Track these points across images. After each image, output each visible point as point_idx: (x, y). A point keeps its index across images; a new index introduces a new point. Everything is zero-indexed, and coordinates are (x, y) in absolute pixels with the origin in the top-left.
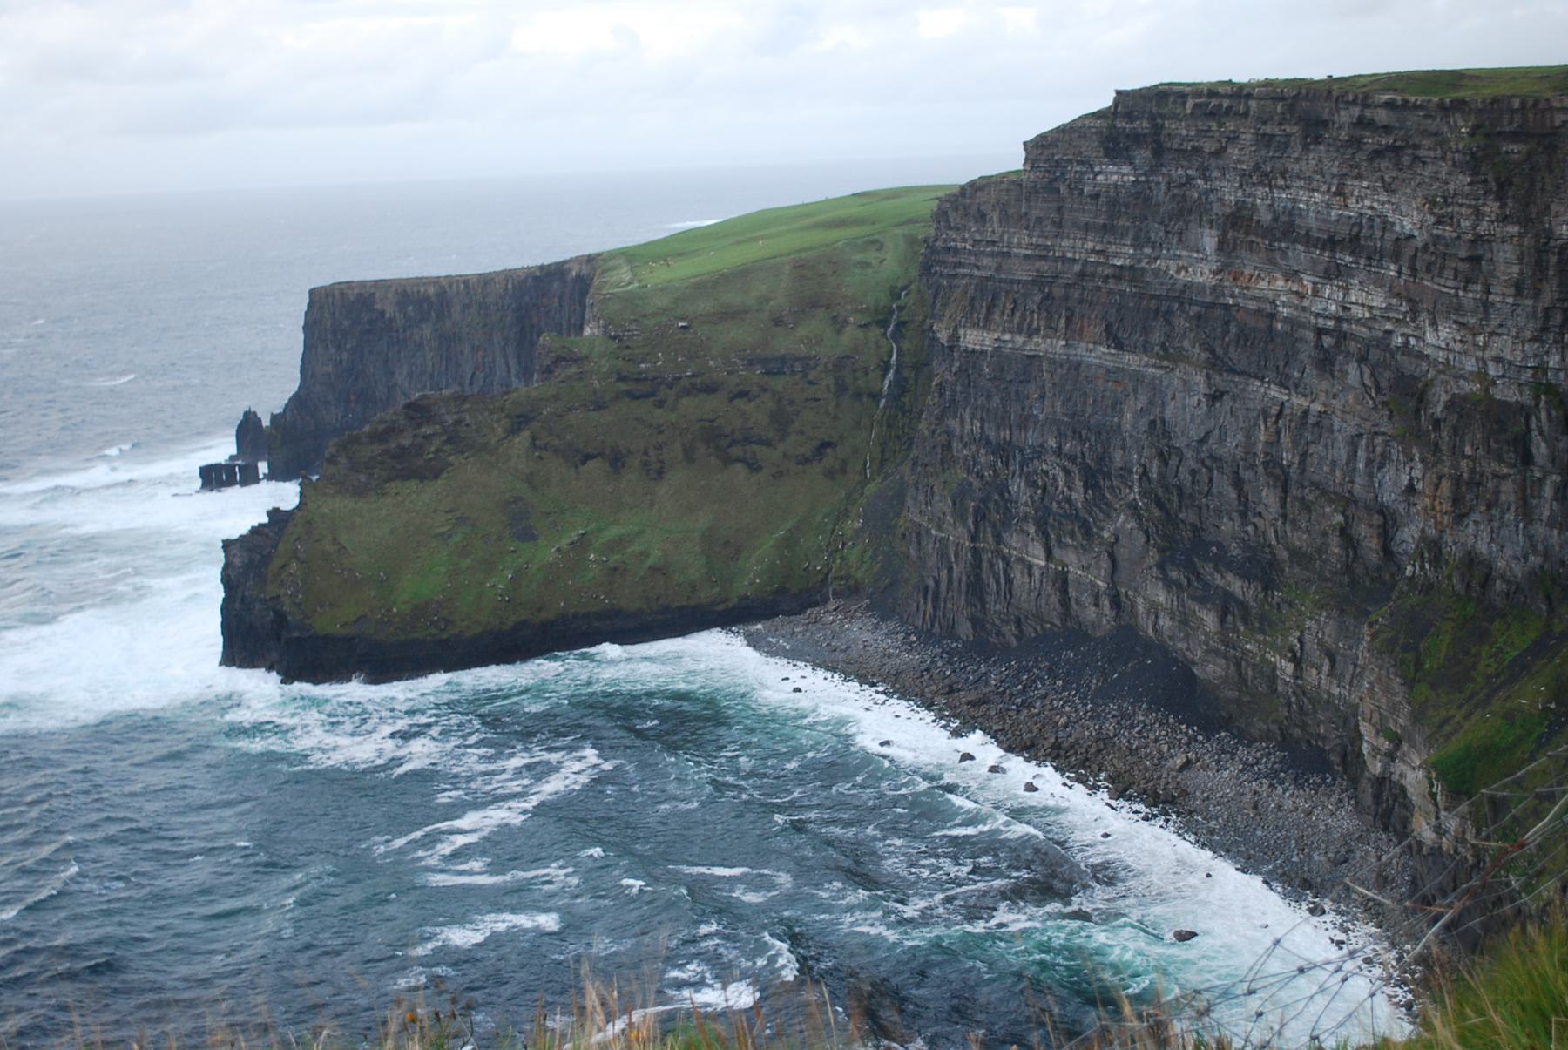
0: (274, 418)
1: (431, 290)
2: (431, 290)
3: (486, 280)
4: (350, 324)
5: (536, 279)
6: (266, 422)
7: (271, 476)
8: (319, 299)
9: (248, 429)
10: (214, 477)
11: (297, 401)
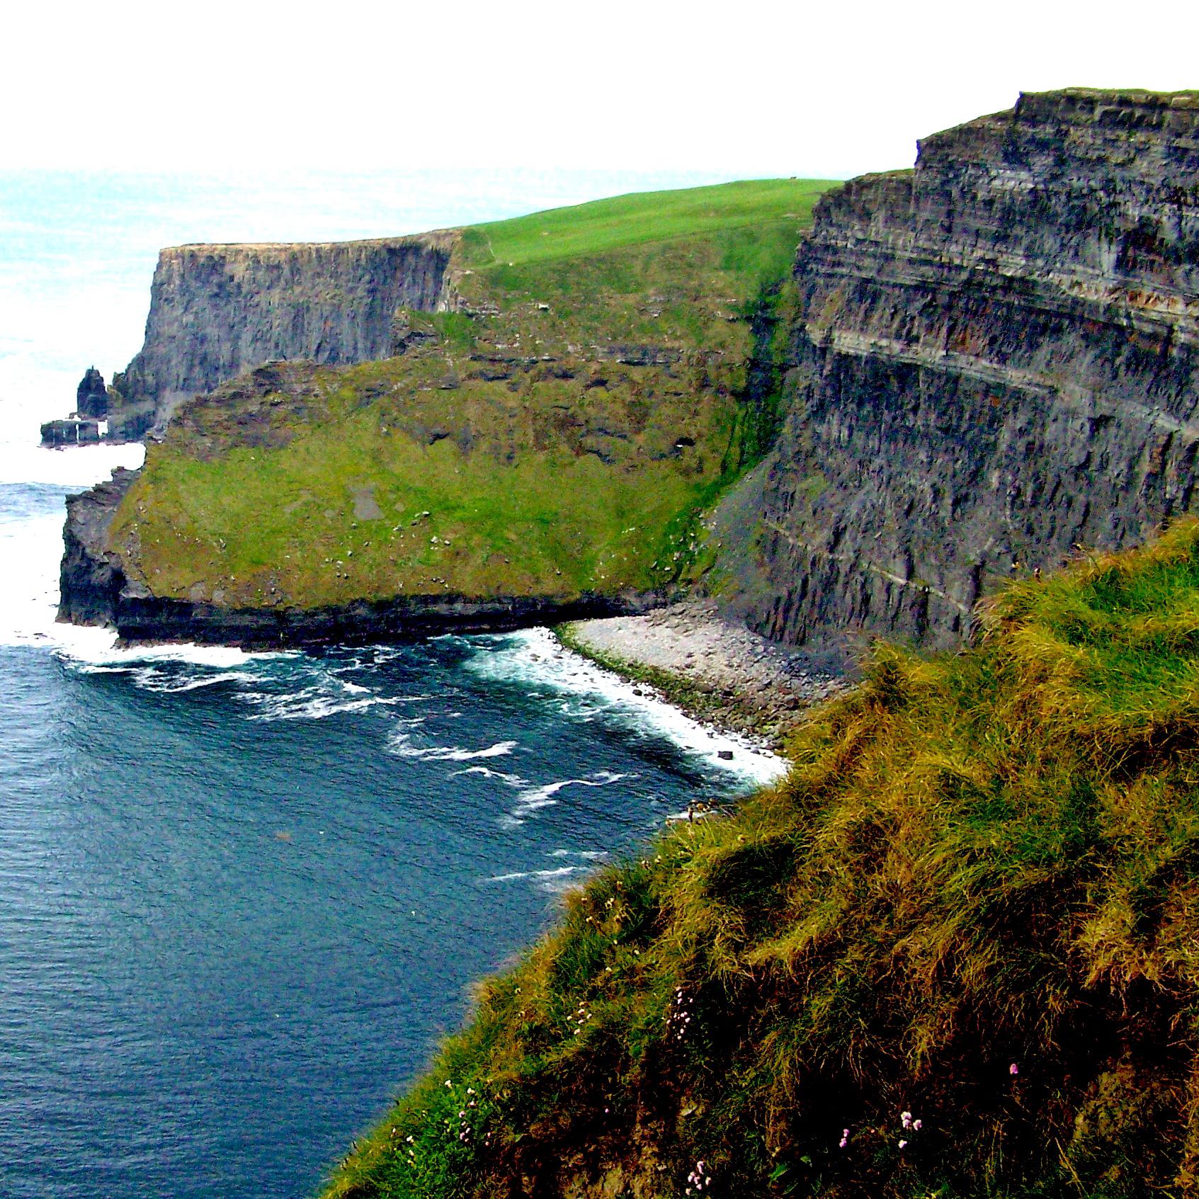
0: (117, 378)
1: (283, 257)
5: (391, 251)
6: (108, 382)
7: (111, 438)
8: (165, 260)
9: (90, 387)
10: (54, 436)
11: (140, 362)
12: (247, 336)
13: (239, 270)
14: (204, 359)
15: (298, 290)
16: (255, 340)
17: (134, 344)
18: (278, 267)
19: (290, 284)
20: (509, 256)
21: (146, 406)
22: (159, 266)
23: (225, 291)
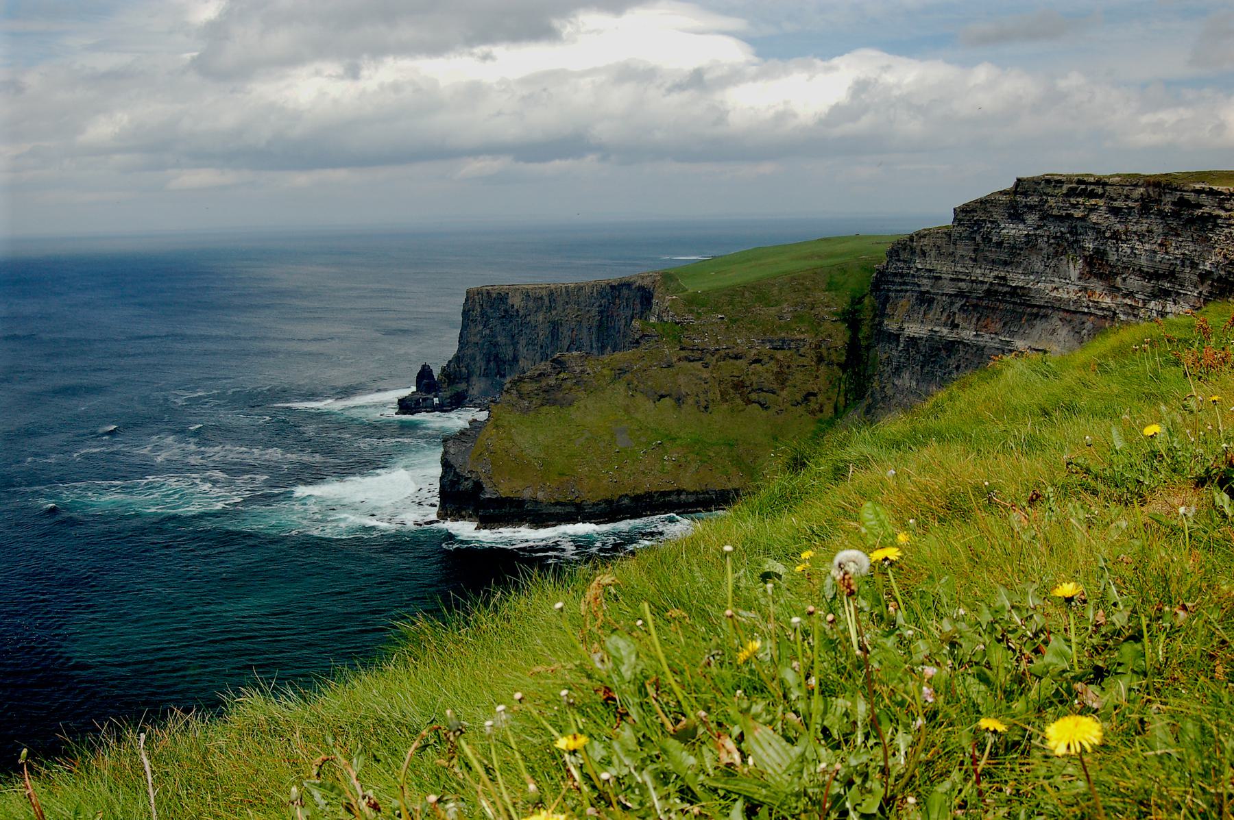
0: (443, 369)
1: (544, 293)
2: (544, 293)
3: (580, 288)
4: (488, 313)
5: (613, 287)
9: (424, 377)
11: (458, 359)
12: (523, 342)
13: (516, 301)
14: (496, 356)
15: (554, 313)
16: (528, 344)
17: (452, 350)
18: (541, 298)
19: (550, 309)
20: (695, 287)
21: (463, 386)
22: (466, 300)
23: (508, 315)
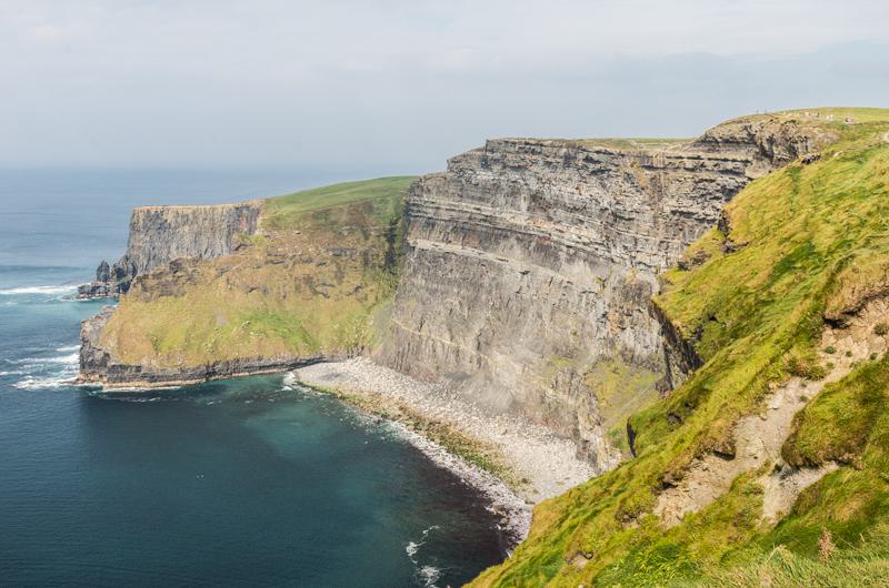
1: (190, 211)
12: (174, 246)
